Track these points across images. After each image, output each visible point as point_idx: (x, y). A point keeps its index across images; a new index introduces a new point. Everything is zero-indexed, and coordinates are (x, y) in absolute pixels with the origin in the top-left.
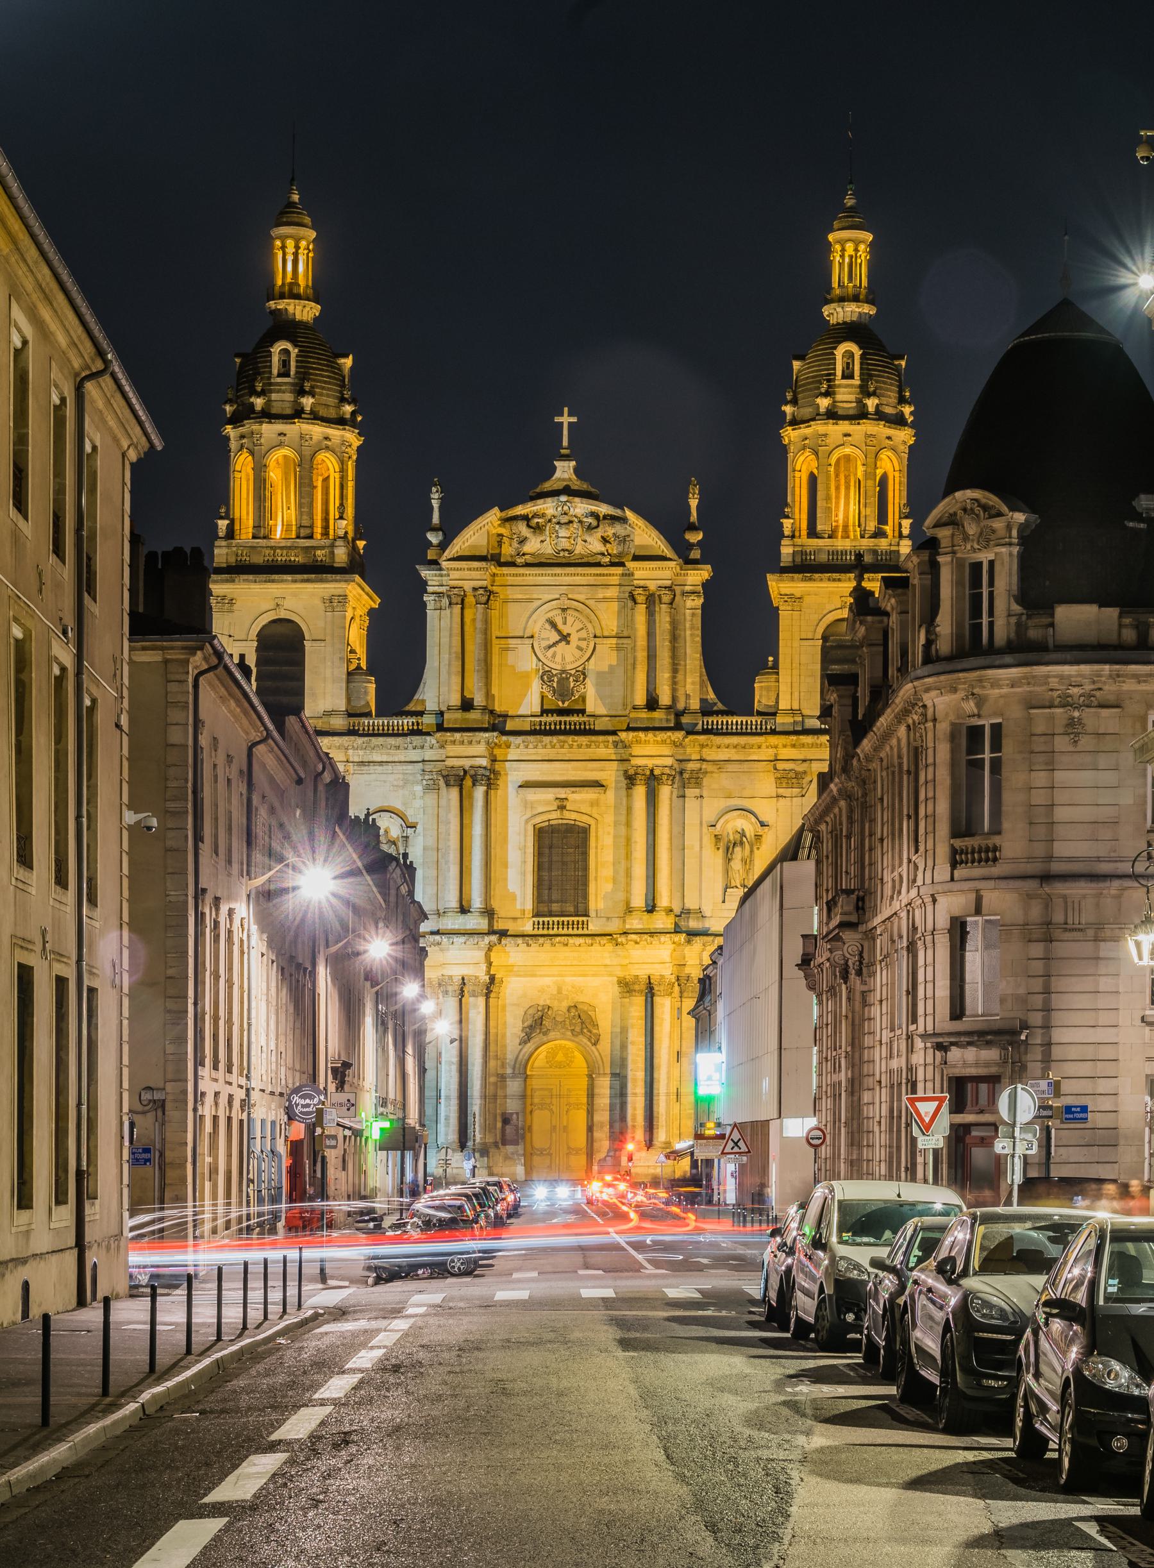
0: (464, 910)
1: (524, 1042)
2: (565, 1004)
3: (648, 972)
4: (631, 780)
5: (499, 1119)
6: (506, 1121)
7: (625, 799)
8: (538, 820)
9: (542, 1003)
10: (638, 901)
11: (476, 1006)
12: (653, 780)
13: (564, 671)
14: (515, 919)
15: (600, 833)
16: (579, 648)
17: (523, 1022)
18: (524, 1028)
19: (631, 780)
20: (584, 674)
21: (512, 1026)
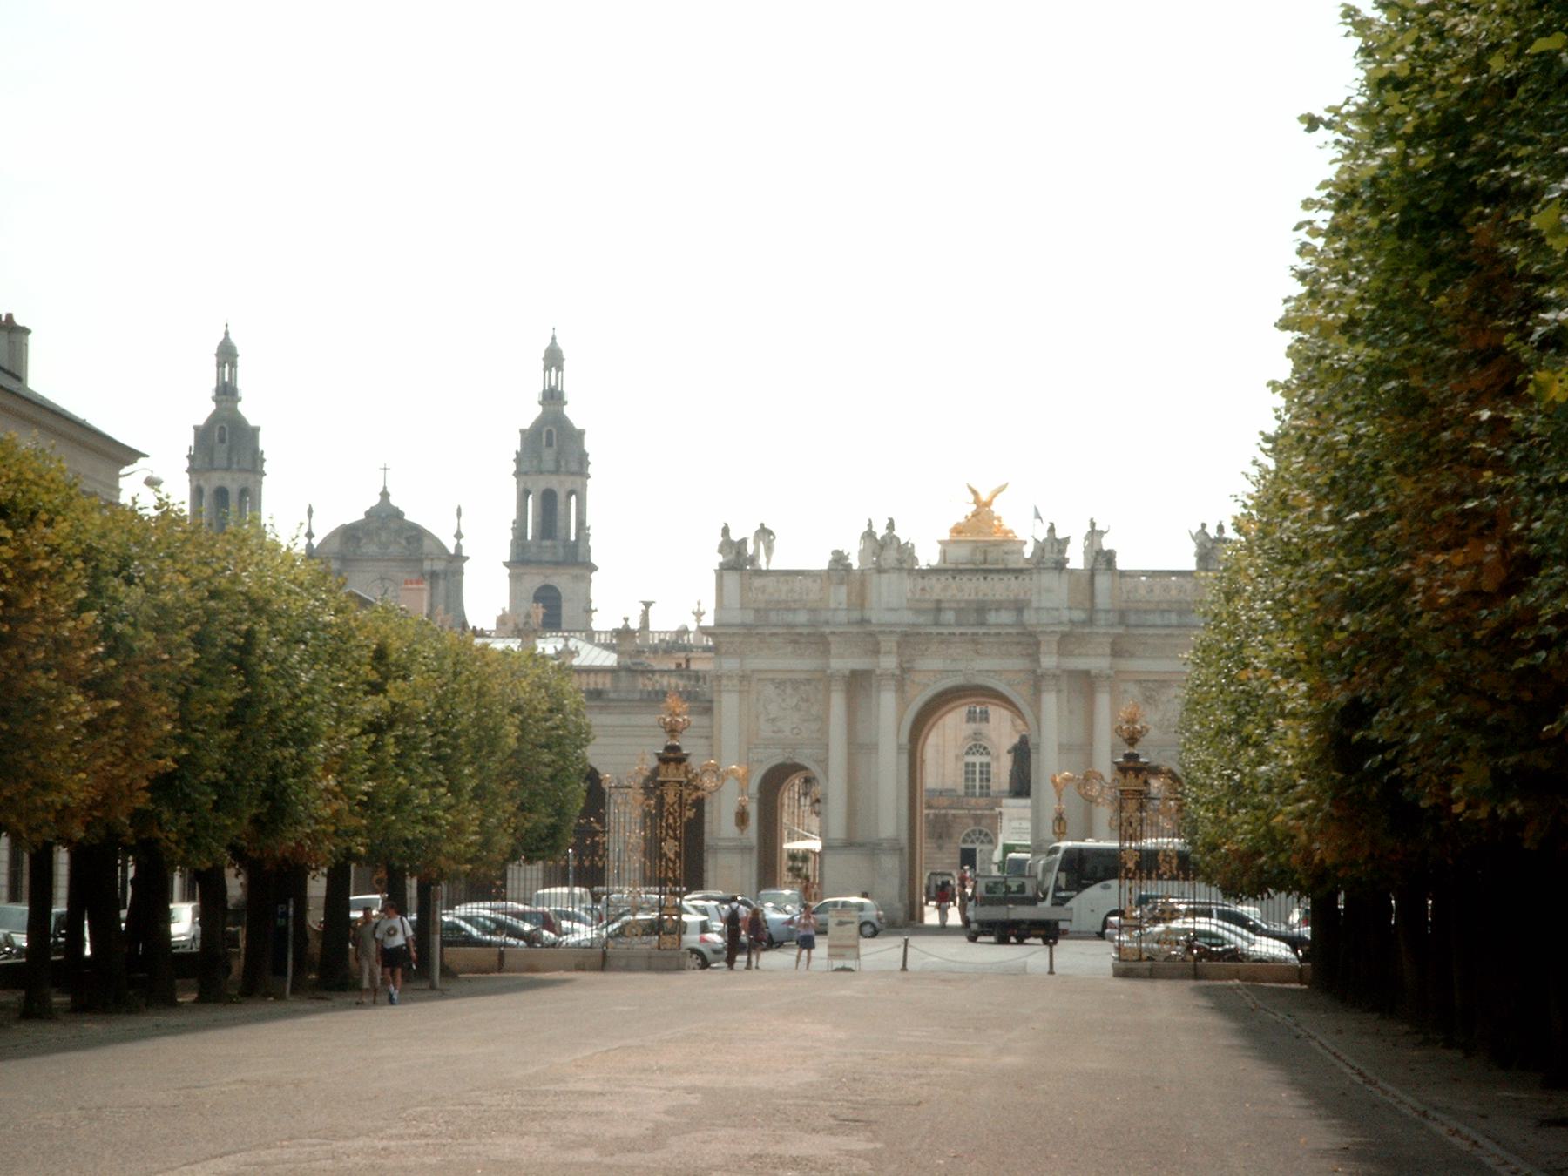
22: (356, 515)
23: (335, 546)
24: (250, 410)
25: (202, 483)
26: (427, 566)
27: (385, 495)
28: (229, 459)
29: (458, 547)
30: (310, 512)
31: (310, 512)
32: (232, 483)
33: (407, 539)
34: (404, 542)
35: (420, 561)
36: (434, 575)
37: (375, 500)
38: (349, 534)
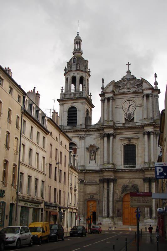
0: (108, 163)
1: (122, 193)
2: (131, 185)
3: (150, 177)
4: (144, 134)
5: (117, 211)
6: (118, 211)
7: (143, 140)
8: (125, 144)
9: (126, 184)
10: (147, 160)
11: (111, 185)
12: (149, 134)
13: (129, 113)
14: (120, 166)
15: (138, 147)
16: (133, 108)
17: (122, 189)
18: (122, 190)
19: (144, 134)
20: (134, 114)
21: (119, 189)
22: (118, 78)
23: (111, 88)
24: (85, 56)
25: (68, 76)
26: (145, 92)
27: (129, 72)
28: (77, 67)
29: (156, 87)
30: (103, 81)
31: (103, 81)
32: (78, 75)
33: (137, 85)
34: (136, 86)
35: (142, 92)
36: (148, 96)
37: (125, 74)
38: (116, 85)
